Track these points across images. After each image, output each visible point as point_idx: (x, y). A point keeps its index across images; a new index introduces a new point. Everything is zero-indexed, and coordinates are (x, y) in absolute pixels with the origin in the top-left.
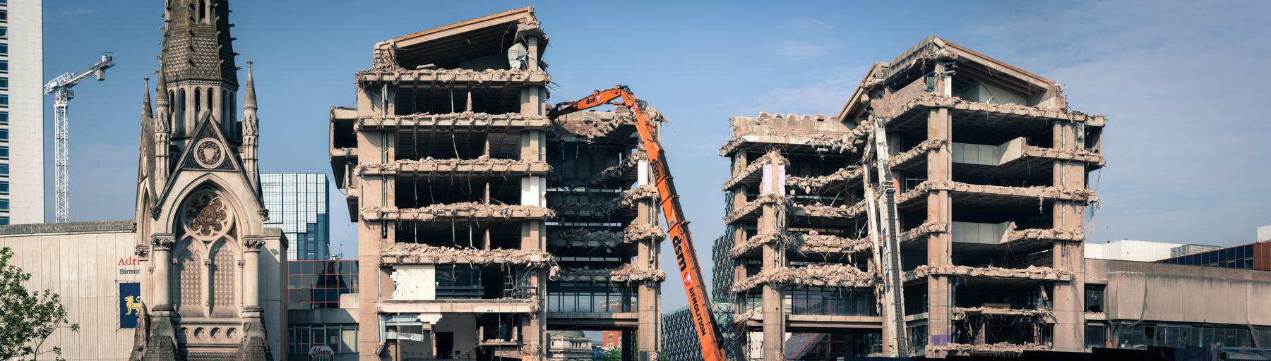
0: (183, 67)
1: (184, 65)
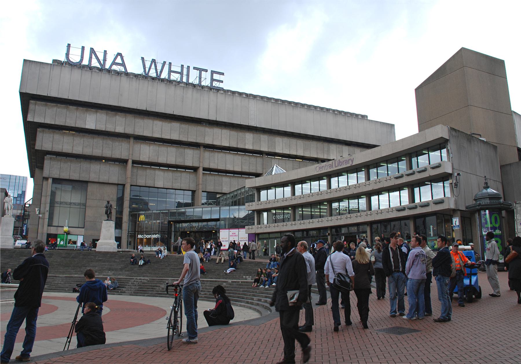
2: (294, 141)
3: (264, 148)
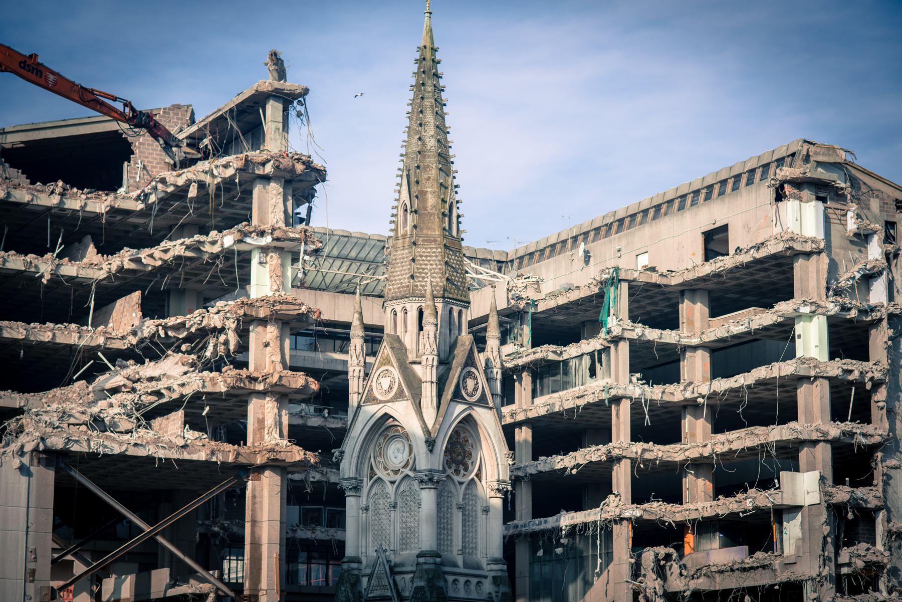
0: (437, 282)
1: (438, 280)
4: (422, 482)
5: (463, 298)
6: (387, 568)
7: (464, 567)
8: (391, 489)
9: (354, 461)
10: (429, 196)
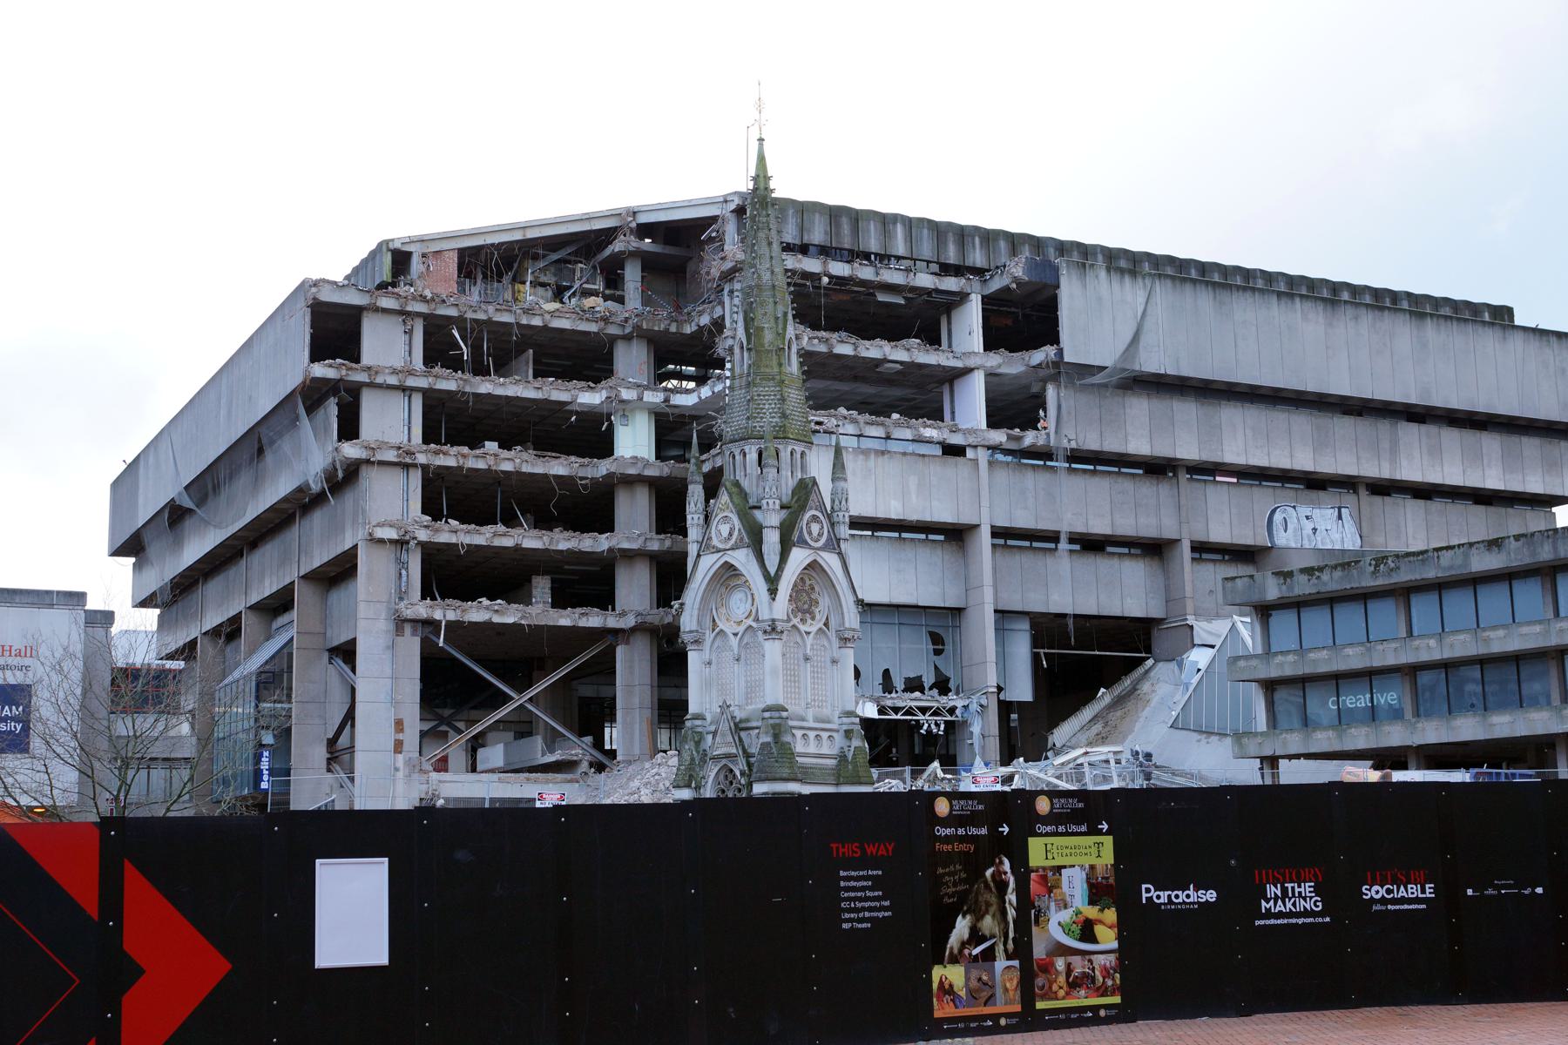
0: (776, 422)
1: (778, 420)
2: (1279, 418)
3: (1188, 450)
4: (765, 632)
5: (806, 439)
6: (732, 724)
7: (814, 722)
8: (734, 642)
9: (696, 612)
10: (766, 332)
